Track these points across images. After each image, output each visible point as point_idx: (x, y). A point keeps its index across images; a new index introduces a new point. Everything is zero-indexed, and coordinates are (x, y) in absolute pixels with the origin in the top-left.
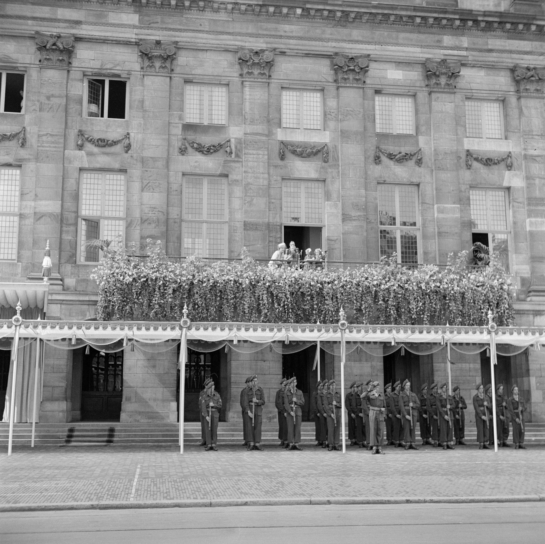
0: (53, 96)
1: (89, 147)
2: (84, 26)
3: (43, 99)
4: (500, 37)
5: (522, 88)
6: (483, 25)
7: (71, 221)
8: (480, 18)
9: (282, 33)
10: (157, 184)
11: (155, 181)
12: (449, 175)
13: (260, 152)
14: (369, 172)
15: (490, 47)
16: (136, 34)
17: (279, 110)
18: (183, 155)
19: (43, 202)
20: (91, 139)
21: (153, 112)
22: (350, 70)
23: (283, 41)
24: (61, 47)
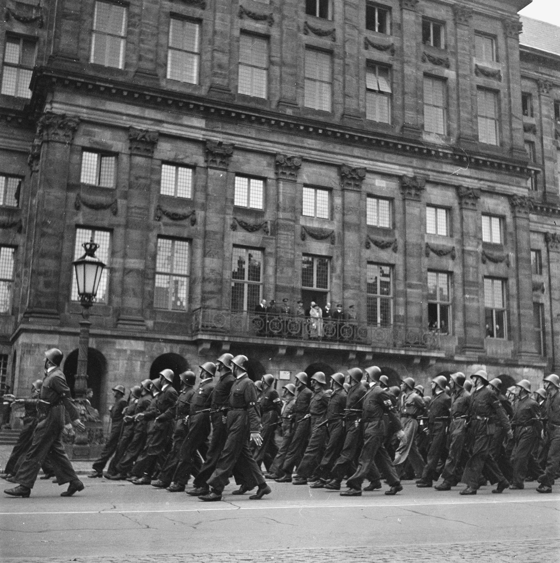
0: (140, 177)
1: (165, 219)
2: (165, 125)
3: (132, 179)
4: (451, 164)
5: (463, 201)
7: (150, 276)
8: (440, 150)
9: (306, 145)
13: (289, 233)
14: (362, 254)
15: (444, 170)
17: (301, 202)
19: (133, 261)
22: (351, 178)
23: (308, 151)
24: (148, 139)
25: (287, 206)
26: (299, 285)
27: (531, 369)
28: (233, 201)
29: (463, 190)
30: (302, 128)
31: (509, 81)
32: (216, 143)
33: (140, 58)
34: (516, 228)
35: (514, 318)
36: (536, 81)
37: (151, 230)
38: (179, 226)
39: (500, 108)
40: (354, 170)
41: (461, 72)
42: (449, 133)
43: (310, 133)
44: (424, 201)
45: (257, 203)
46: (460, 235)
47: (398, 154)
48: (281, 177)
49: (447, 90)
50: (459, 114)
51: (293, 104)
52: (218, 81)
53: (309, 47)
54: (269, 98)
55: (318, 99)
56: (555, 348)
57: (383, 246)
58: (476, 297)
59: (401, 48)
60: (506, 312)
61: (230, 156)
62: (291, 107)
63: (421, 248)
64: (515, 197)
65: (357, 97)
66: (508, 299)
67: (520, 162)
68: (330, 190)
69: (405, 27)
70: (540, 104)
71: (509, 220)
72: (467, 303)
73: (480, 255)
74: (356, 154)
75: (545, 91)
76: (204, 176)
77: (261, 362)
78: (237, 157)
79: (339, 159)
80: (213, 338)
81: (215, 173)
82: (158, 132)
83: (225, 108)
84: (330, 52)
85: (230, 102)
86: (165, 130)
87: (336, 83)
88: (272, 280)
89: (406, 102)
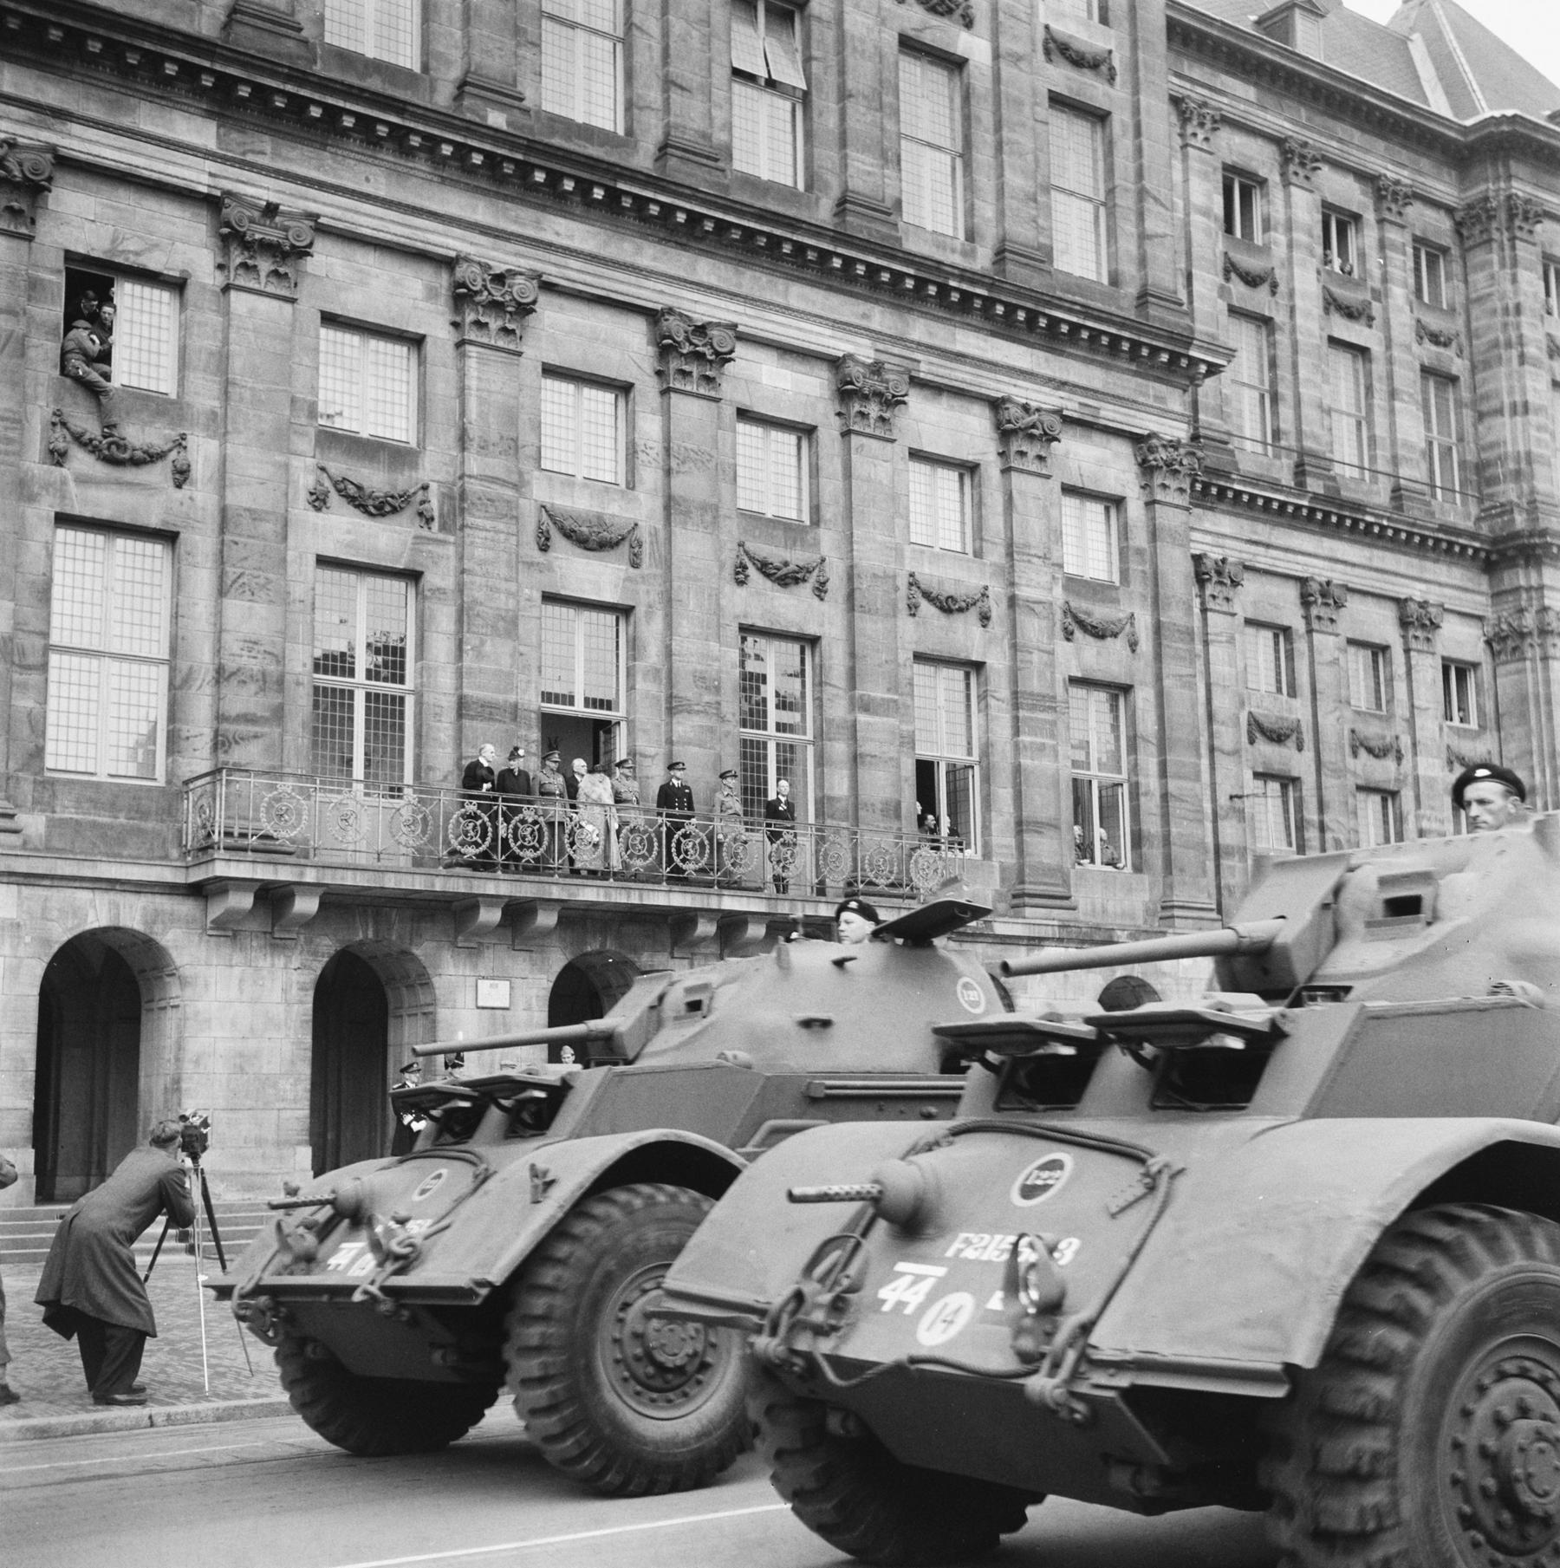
2: (76, 129)
4: (978, 329)
6: (955, 297)
8: (953, 283)
9: (548, 236)
10: (262, 581)
11: (256, 573)
12: (880, 625)
13: (501, 526)
14: (723, 602)
16: (211, 174)
18: (318, 509)
20: (91, 440)
21: (252, 389)
22: (689, 354)
25: (494, 438)
27: (1199, 959)
28: (313, 413)
29: (1014, 411)
30: (540, 177)
31: (1136, 91)
32: (254, 206)
34: (1154, 535)
35: (1150, 805)
37: (32, 498)
38: (130, 484)
39: (1110, 171)
40: (701, 330)
41: (1006, 44)
42: (971, 236)
43: (564, 196)
45: (393, 422)
46: (1002, 550)
47: (830, 288)
48: (472, 335)
50: (1001, 175)
51: (508, 97)
54: (426, 68)
56: (1225, 892)
57: (787, 578)
58: (1052, 742)
60: (1126, 786)
61: (302, 253)
62: (502, 107)
63: (896, 589)
64: (1154, 442)
66: (1133, 748)
67: (1171, 337)
68: (624, 389)
70: (1186, 171)
72: (1025, 761)
73: (1059, 615)
74: (705, 279)
75: (1201, 136)
76: (217, 320)
77: (417, 952)
78: (326, 259)
79: (651, 294)
80: (264, 873)
81: (252, 311)
82: (52, 149)
83: (289, 88)
85: (301, 65)
86: (75, 144)
87: (640, 41)
88: (445, 680)
89: (851, 123)
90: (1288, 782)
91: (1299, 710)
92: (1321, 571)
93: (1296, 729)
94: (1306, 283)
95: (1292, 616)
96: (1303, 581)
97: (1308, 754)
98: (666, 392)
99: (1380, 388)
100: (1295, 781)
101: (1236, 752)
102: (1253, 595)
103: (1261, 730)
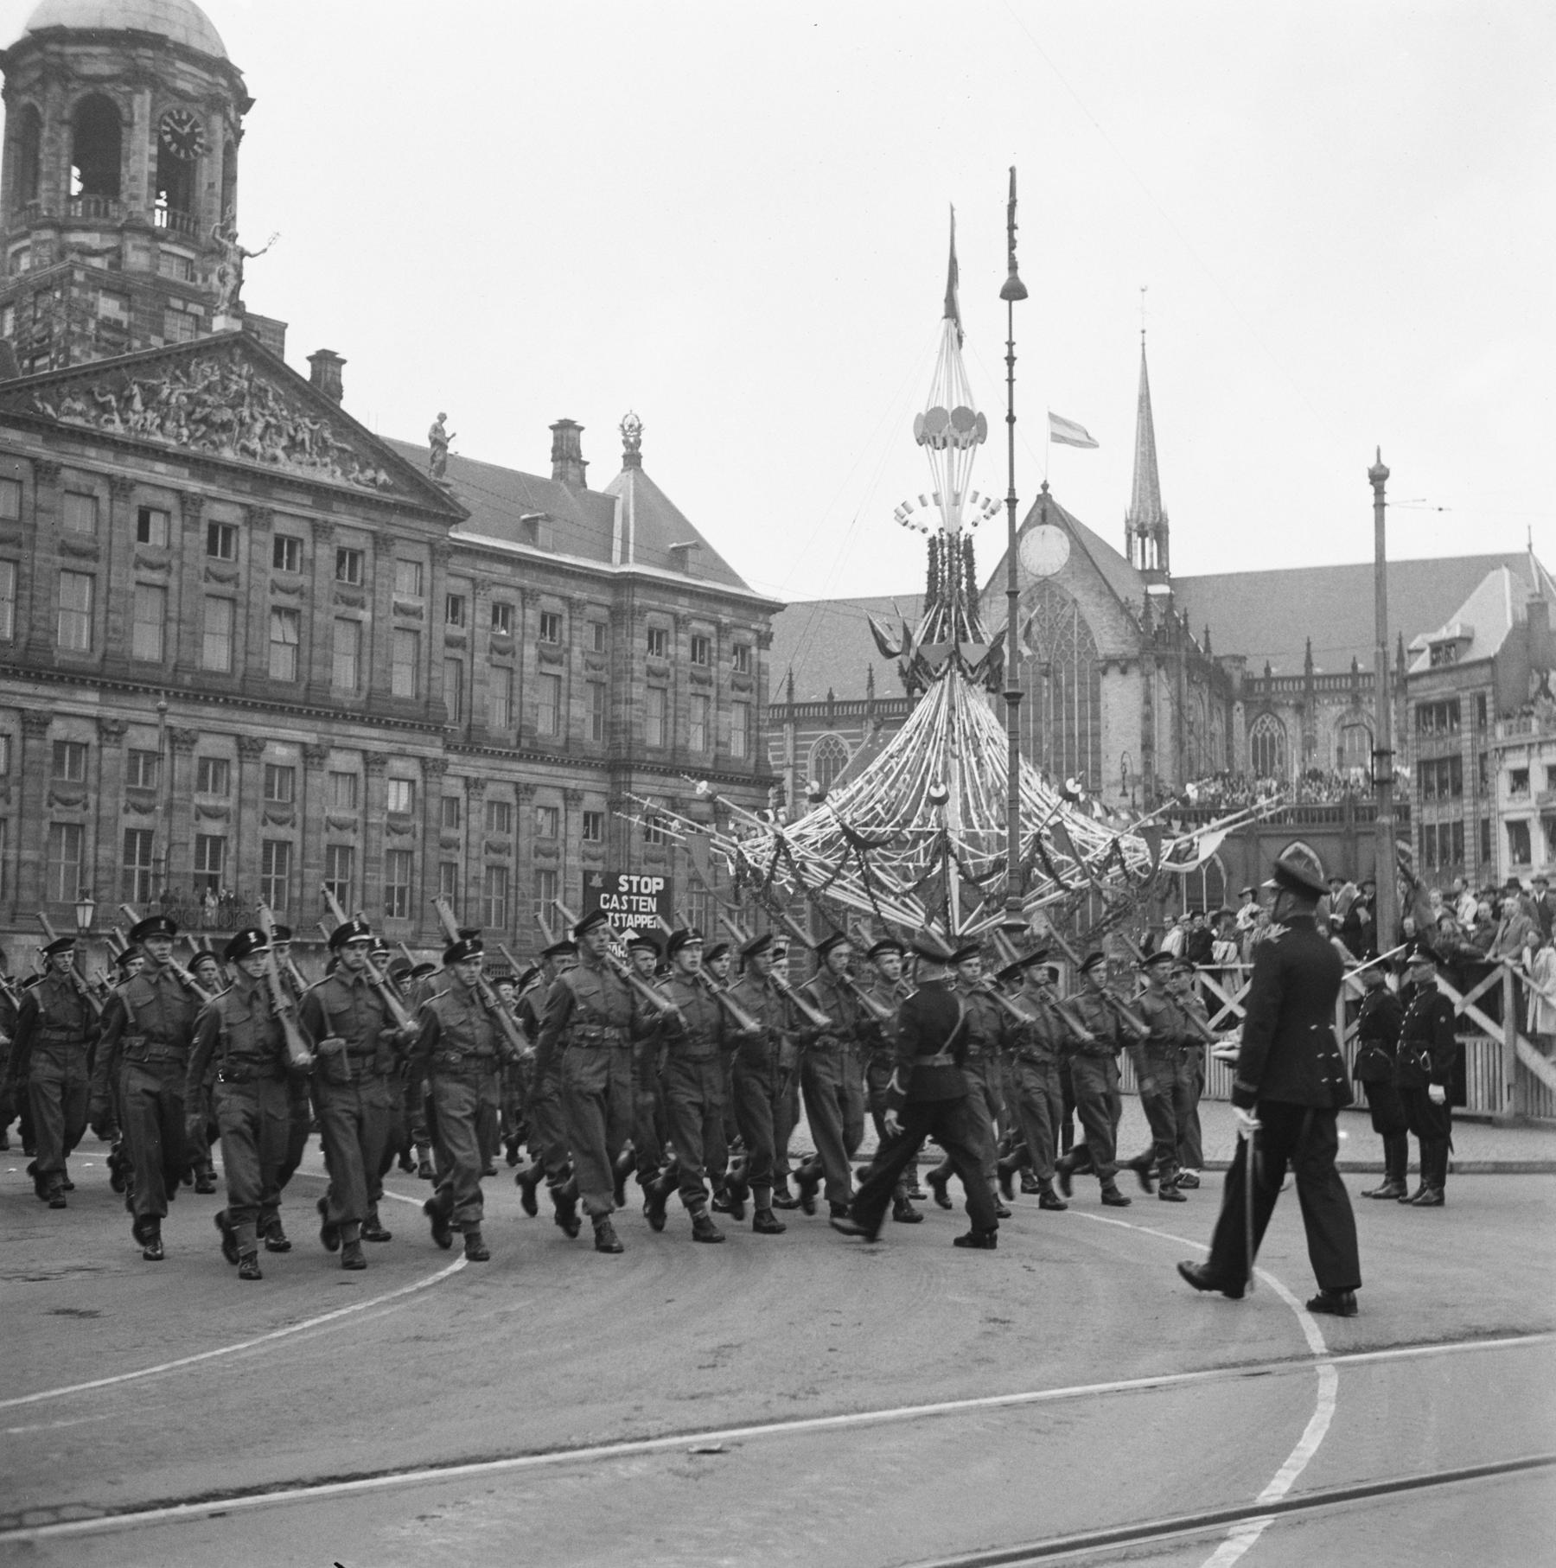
1: (58, 806)
26: (192, 869)
31: (431, 619)
33: (32, 628)
34: (426, 794)
35: (417, 895)
36: (473, 579)
39: (418, 654)
41: (379, 614)
42: (359, 688)
44: (327, 769)
49: (361, 634)
51: (190, 668)
52: (112, 646)
53: (209, 595)
55: (216, 655)
57: (280, 822)
59: (312, 589)
65: (261, 653)
69: (317, 564)
71: (419, 784)
78: (132, 732)
79: (238, 728)
84: (233, 601)
90: (503, 869)
91: (511, 838)
92: (525, 778)
93: (509, 847)
94: (530, 651)
95: (512, 799)
96: (517, 784)
97: (513, 858)
98: (241, 762)
99: (564, 692)
100: (507, 869)
101: (478, 859)
102: (491, 791)
103: (489, 847)
